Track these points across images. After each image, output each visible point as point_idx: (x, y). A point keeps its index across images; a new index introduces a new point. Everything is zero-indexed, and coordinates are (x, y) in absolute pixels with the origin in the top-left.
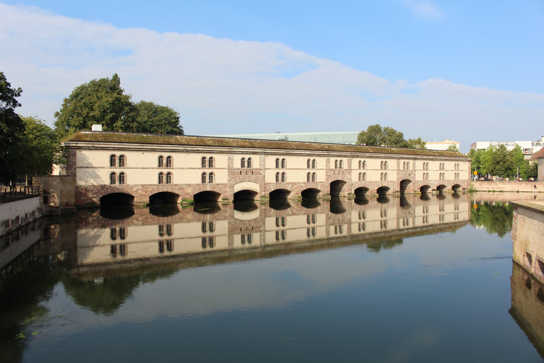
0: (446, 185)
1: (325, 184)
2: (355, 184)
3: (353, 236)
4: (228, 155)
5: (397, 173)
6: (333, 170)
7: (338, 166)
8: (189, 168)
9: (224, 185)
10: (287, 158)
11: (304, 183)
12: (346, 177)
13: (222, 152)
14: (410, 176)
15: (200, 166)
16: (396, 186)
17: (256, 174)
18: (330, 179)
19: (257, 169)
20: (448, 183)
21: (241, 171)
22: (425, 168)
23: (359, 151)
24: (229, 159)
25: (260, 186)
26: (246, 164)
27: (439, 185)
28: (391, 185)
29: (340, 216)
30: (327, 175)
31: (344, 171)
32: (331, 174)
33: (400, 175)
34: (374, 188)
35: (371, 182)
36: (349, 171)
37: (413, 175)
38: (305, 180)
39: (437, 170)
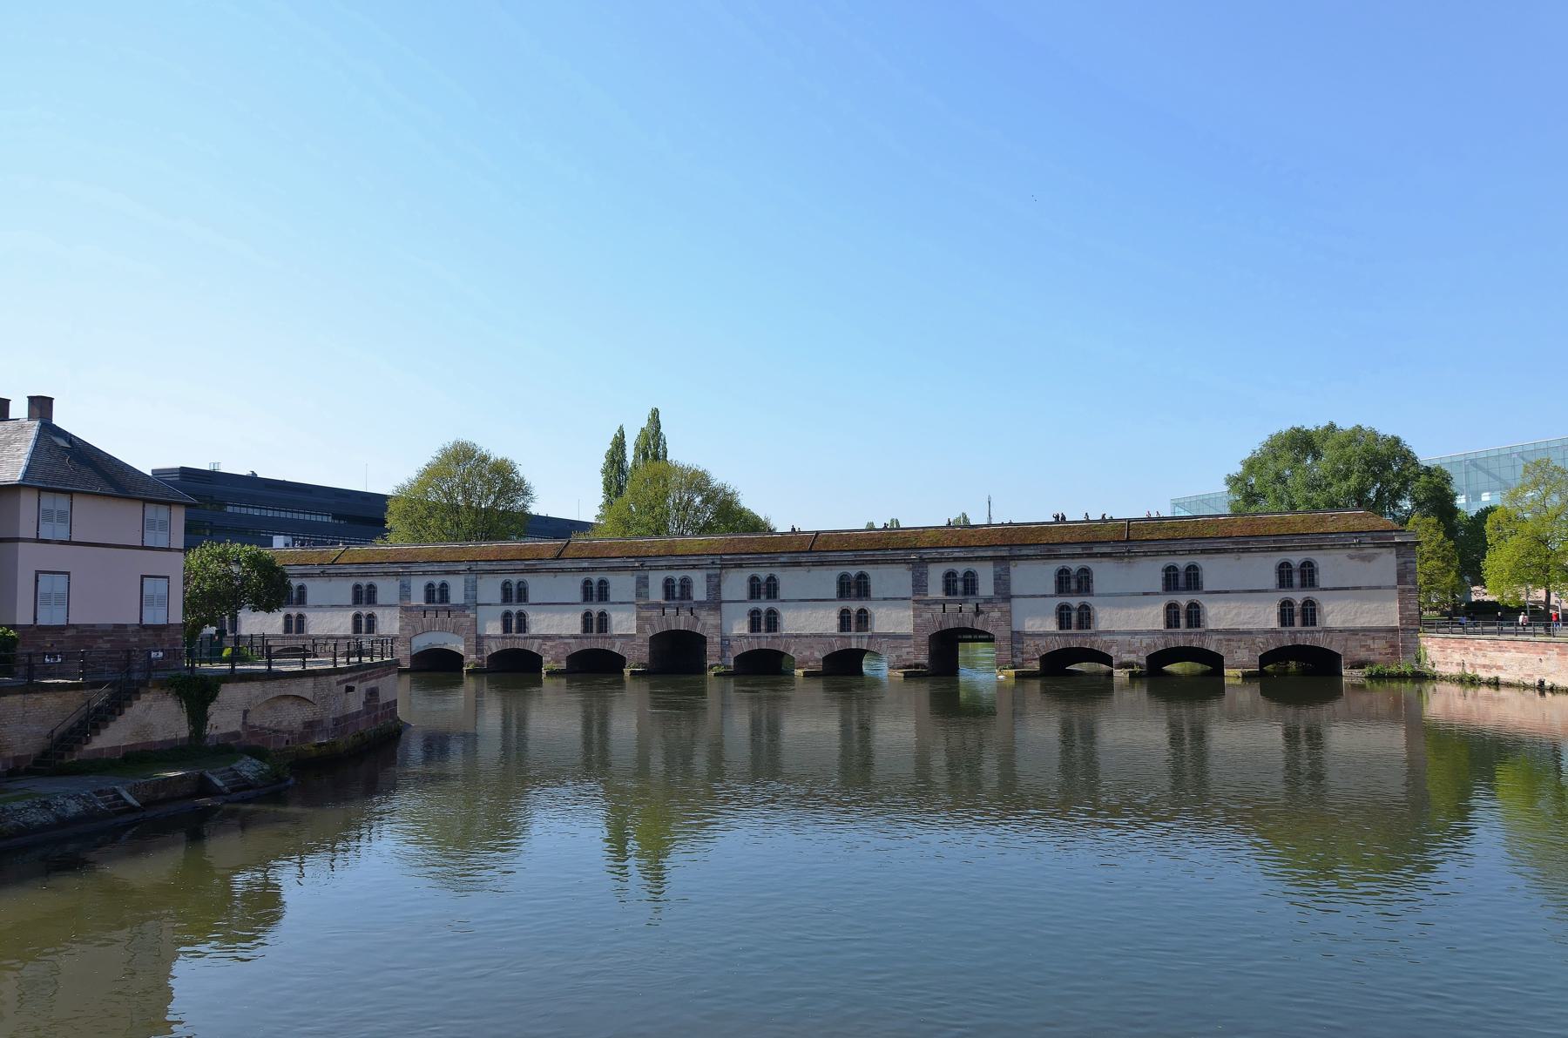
0: (1213, 649)
10: (527, 578)
11: (575, 637)
13: (386, 574)
14: (981, 617)
15: (349, 601)
16: (912, 650)
20: (1229, 640)
22: (1074, 586)
23: (743, 552)
24: (403, 586)
26: (437, 596)
28: (884, 646)
30: (638, 618)
33: (927, 615)
34: (812, 654)
35: (797, 636)
37: (996, 614)
38: (578, 631)
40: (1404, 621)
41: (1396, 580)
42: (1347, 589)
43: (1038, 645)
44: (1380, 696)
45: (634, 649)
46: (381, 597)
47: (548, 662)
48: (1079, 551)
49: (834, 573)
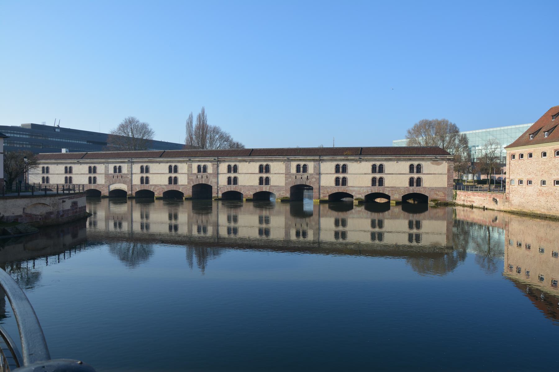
0: (387, 193)
1: (186, 187)
2: (222, 187)
3: (288, 241)
4: (105, 164)
5: (286, 177)
6: (195, 174)
7: (202, 171)
8: (81, 174)
9: (103, 185)
10: (149, 165)
11: (166, 185)
12: (210, 181)
14: (309, 181)
15: (87, 172)
17: (124, 178)
18: (191, 182)
19: (124, 174)
20: (392, 191)
21: (113, 176)
24: (106, 167)
25: (128, 187)
27: (369, 193)
28: (275, 191)
29: (204, 218)
30: (188, 179)
31: (208, 175)
32: (194, 178)
34: (249, 193)
35: (244, 186)
36: (214, 175)
37: (314, 180)
38: (167, 182)
39: (365, 174)
40: (449, 186)
41: (447, 172)
42: (431, 174)
43: (328, 191)
44: (440, 211)
45: (186, 190)
46: (98, 171)
47: (156, 195)
48: (343, 158)
49: (258, 164)
